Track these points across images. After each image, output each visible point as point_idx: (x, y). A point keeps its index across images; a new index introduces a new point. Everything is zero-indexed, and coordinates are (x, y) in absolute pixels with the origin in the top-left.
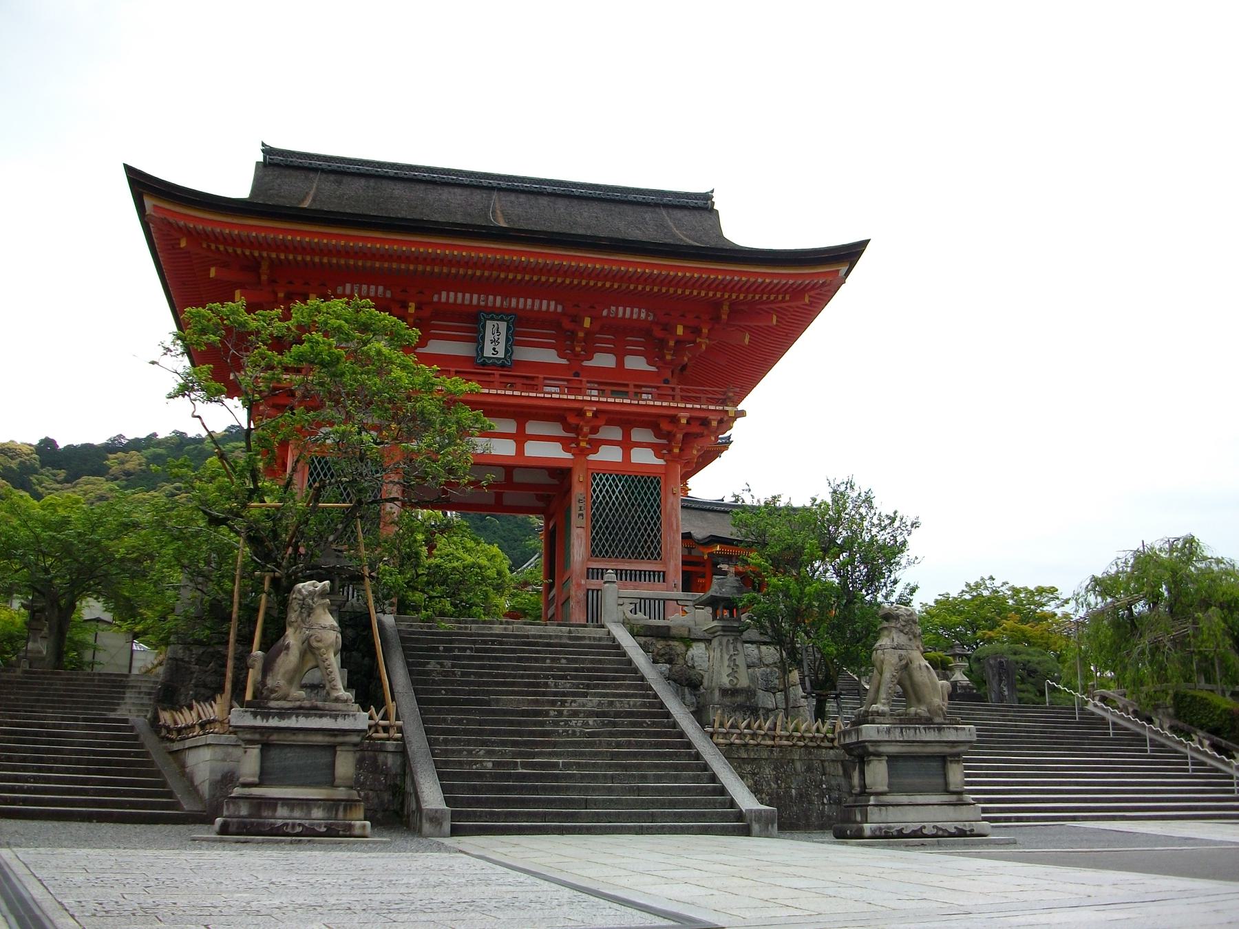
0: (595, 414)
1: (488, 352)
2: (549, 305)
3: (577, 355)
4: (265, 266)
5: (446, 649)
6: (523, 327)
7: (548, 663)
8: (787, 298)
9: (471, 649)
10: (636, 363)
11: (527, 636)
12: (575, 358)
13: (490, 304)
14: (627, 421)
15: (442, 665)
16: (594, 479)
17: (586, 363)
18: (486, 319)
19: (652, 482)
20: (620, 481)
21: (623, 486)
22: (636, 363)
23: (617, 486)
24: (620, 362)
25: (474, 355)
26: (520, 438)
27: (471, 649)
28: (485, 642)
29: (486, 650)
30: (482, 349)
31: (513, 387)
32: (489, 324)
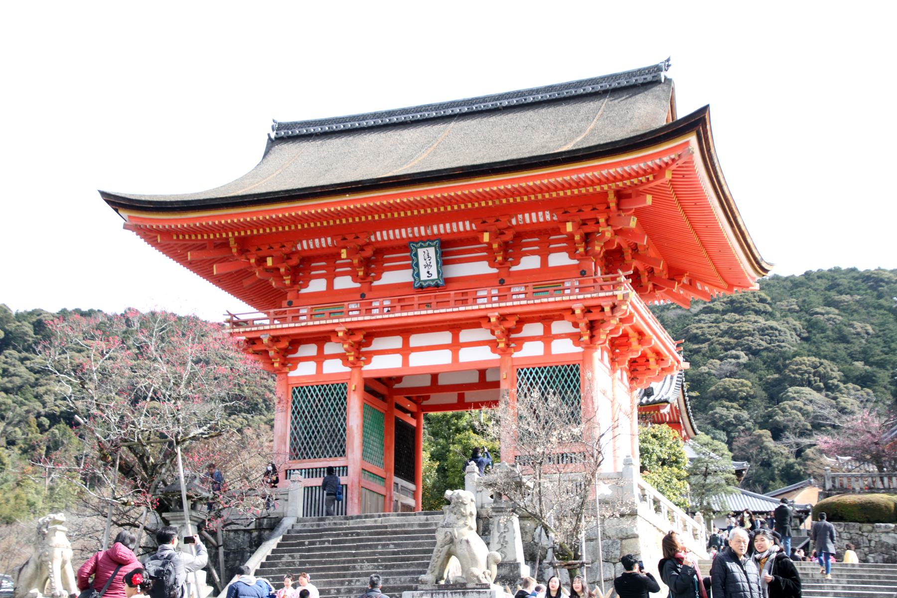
0: (503, 318)
1: (424, 276)
2: (464, 226)
3: (500, 264)
4: (232, 242)
5: (311, 543)
6: (448, 250)
7: (380, 549)
8: (651, 177)
9: (329, 541)
10: (559, 259)
11: (386, 527)
12: (501, 265)
13: (417, 235)
14: (547, 318)
15: (293, 557)
16: (520, 374)
17: (514, 268)
18: (417, 248)
19: (571, 370)
20: (542, 372)
21: (545, 378)
22: (559, 259)
23: (540, 378)
24: (544, 262)
25: (412, 280)
26: (455, 346)
27: (329, 541)
28: (346, 535)
29: (340, 542)
30: (418, 275)
31: (429, 305)
32: (420, 252)
